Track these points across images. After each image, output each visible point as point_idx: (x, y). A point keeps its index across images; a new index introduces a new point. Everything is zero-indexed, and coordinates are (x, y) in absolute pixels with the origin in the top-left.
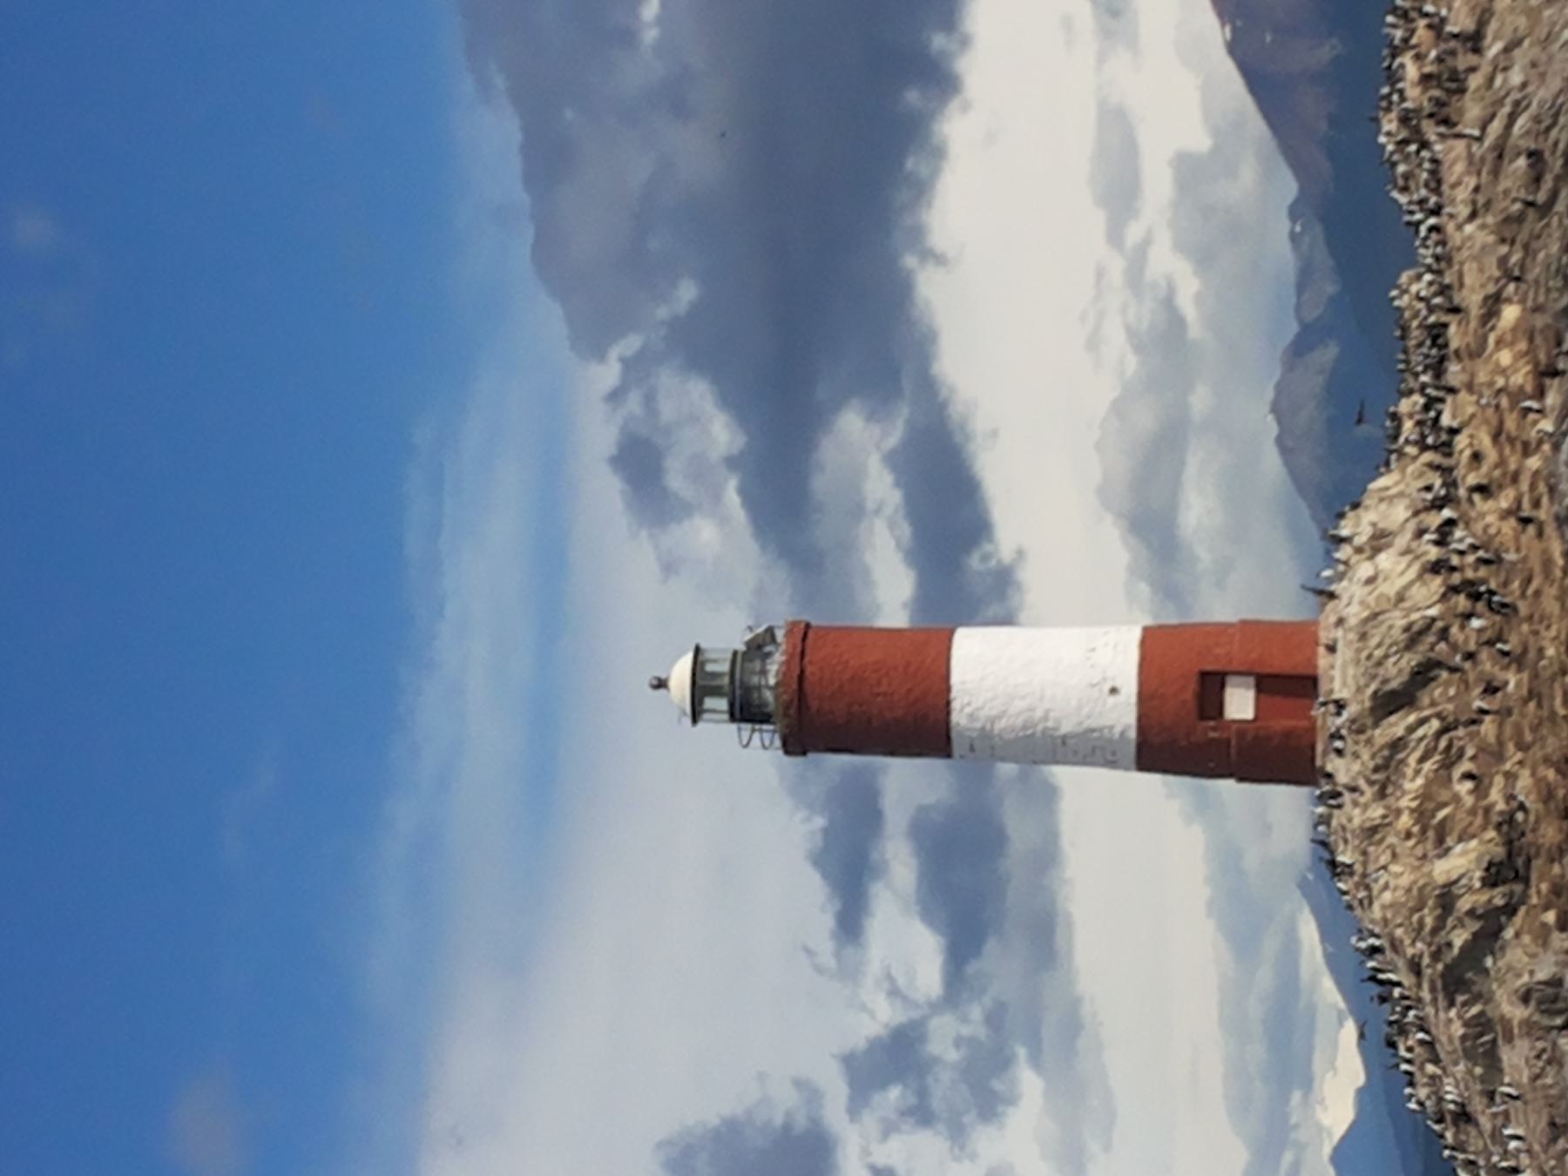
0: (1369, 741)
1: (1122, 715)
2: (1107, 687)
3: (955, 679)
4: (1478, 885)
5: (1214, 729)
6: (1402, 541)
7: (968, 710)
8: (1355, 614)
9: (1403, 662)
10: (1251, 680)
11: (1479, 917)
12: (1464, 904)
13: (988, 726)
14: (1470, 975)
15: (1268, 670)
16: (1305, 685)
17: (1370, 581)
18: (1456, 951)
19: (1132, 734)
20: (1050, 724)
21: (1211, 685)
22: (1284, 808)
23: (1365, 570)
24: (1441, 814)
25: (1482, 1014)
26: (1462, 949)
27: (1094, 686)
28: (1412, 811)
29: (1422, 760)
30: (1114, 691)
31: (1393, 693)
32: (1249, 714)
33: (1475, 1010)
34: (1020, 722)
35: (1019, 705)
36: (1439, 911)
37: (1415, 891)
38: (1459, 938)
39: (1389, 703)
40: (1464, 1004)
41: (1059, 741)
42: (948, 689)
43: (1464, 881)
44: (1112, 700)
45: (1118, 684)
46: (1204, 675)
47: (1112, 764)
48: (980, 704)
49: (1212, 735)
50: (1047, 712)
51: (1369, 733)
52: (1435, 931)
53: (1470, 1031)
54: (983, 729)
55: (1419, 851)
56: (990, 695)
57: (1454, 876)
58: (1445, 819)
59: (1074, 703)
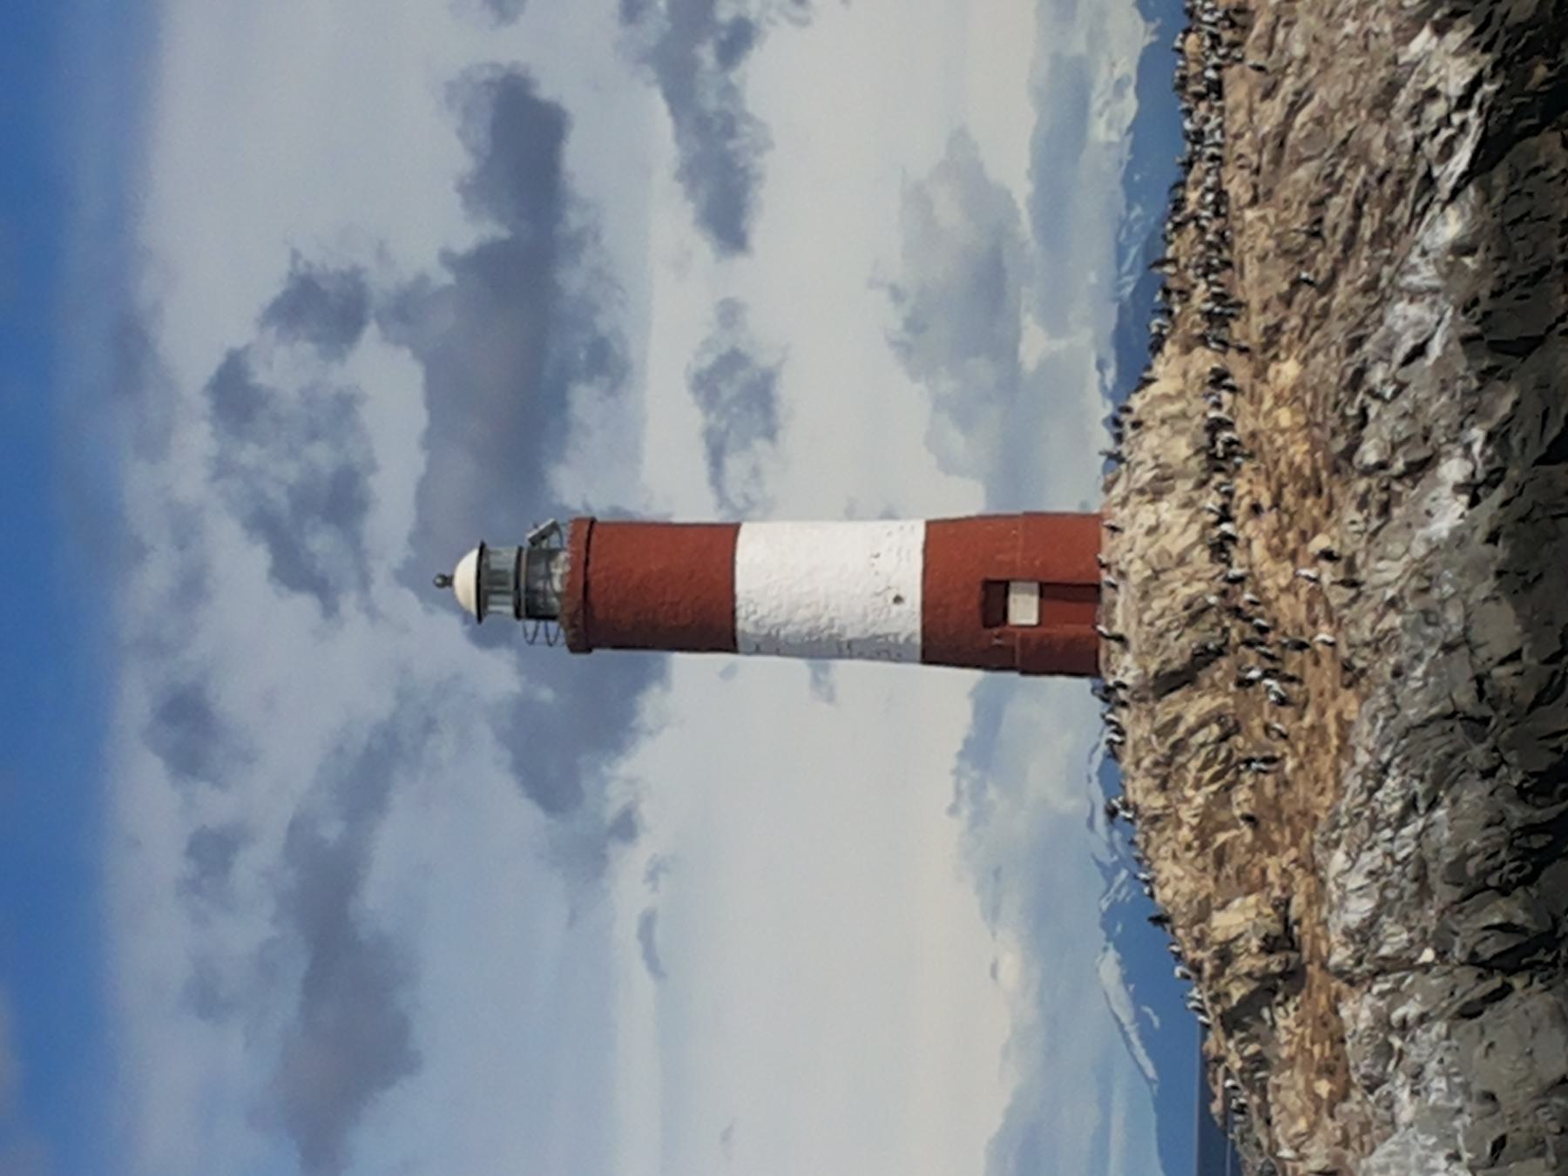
0: (1151, 714)
1: (908, 621)
2: (891, 595)
3: (741, 587)
4: (1255, 950)
5: (998, 637)
6: (1184, 487)
7: (753, 618)
9: (1184, 640)
10: (1035, 586)
11: (1256, 979)
12: (1244, 964)
13: (774, 632)
14: (1246, 1020)
15: (1050, 579)
17: (1152, 531)
18: (1234, 1002)
19: (918, 640)
20: (835, 631)
21: (996, 594)
22: (1073, 691)
23: (1147, 516)
24: (1222, 837)
25: (1259, 1053)
26: (1239, 1002)
27: (878, 594)
28: (1192, 828)
29: (1204, 768)
30: (898, 600)
31: (1174, 674)
32: (1033, 620)
33: (1252, 1049)
34: (805, 629)
35: (803, 614)
36: (1217, 962)
37: (1195, 903)
38: (1237, 992)
39: (1170, 682)
40: (1242, 1041)
41: (844, 646)
42: (732, 597)
43: (1241, 942)
44: (896, 608)
45: (902, 594)
46: (988, 584)
47: (898, 659)
48: (765, 612)
49: (997, 642)
50: (832, 620)
51: (1151, 703)
52: (1213, 977)
53: (1247, 1065)
54: (769, 635)
55: (1200, 862)
56: (775, 603)
57: (1233, 934)
58: (1224, 844)
59: (859, 611)
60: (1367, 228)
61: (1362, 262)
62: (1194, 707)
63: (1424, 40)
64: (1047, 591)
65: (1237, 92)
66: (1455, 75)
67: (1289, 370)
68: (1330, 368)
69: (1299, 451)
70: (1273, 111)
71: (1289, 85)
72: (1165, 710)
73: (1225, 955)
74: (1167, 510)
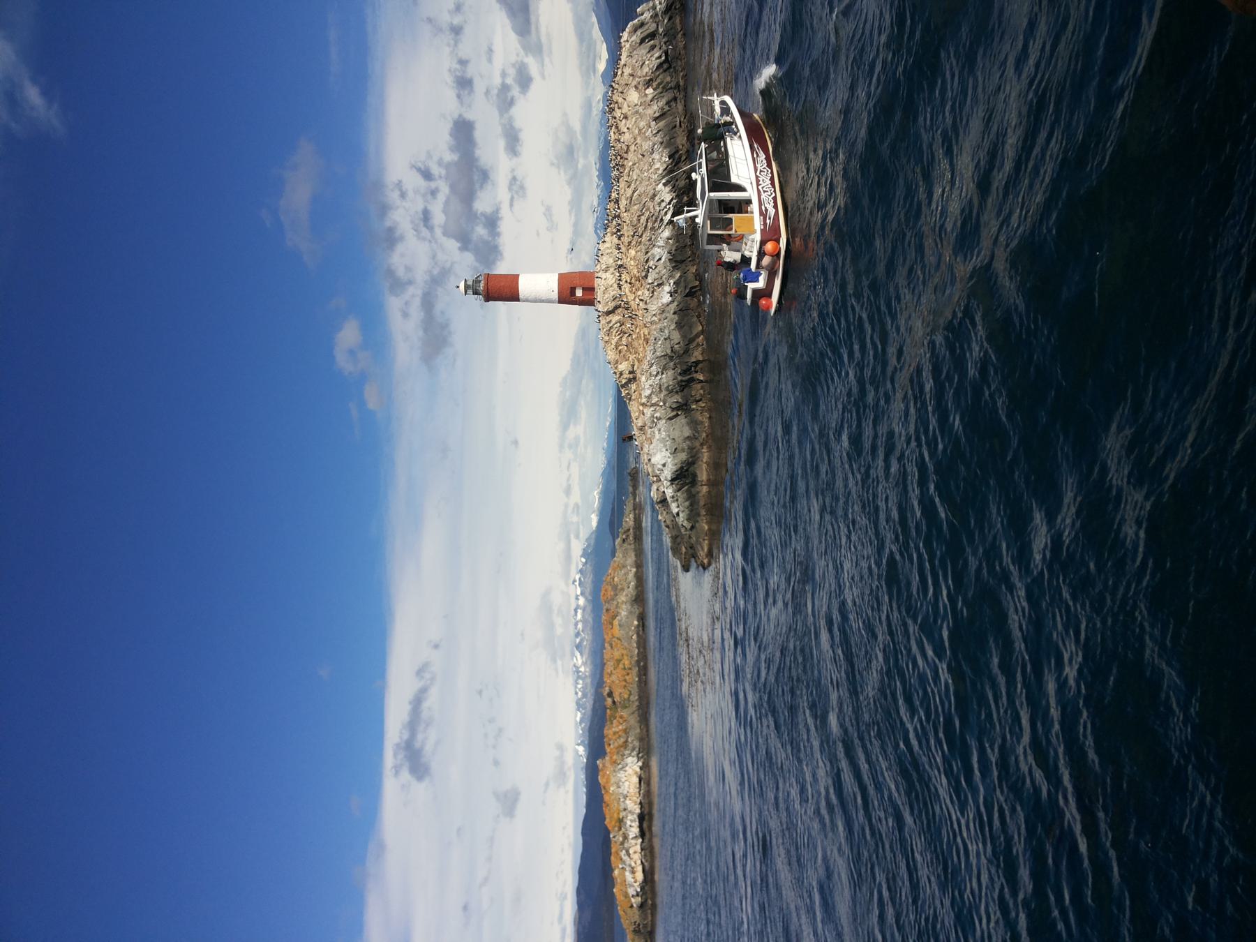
6: (612, 270)
8: (603, 288)
16: (593, 289)
21: (573, 290)
39: (608, 313)
60: (650, 225)
61: (648, 233)
62: (615, 318)
63: (661, 186)
64: (584, 289)
65: (622, 184)
66: (668, 198)
67: (632, 252)
68: (642, 258)
69: (635, 271)
70: (629, 192)
71: (633, 186)
72: (608, 319)
73: (621, 374)
74: (608, 275)
